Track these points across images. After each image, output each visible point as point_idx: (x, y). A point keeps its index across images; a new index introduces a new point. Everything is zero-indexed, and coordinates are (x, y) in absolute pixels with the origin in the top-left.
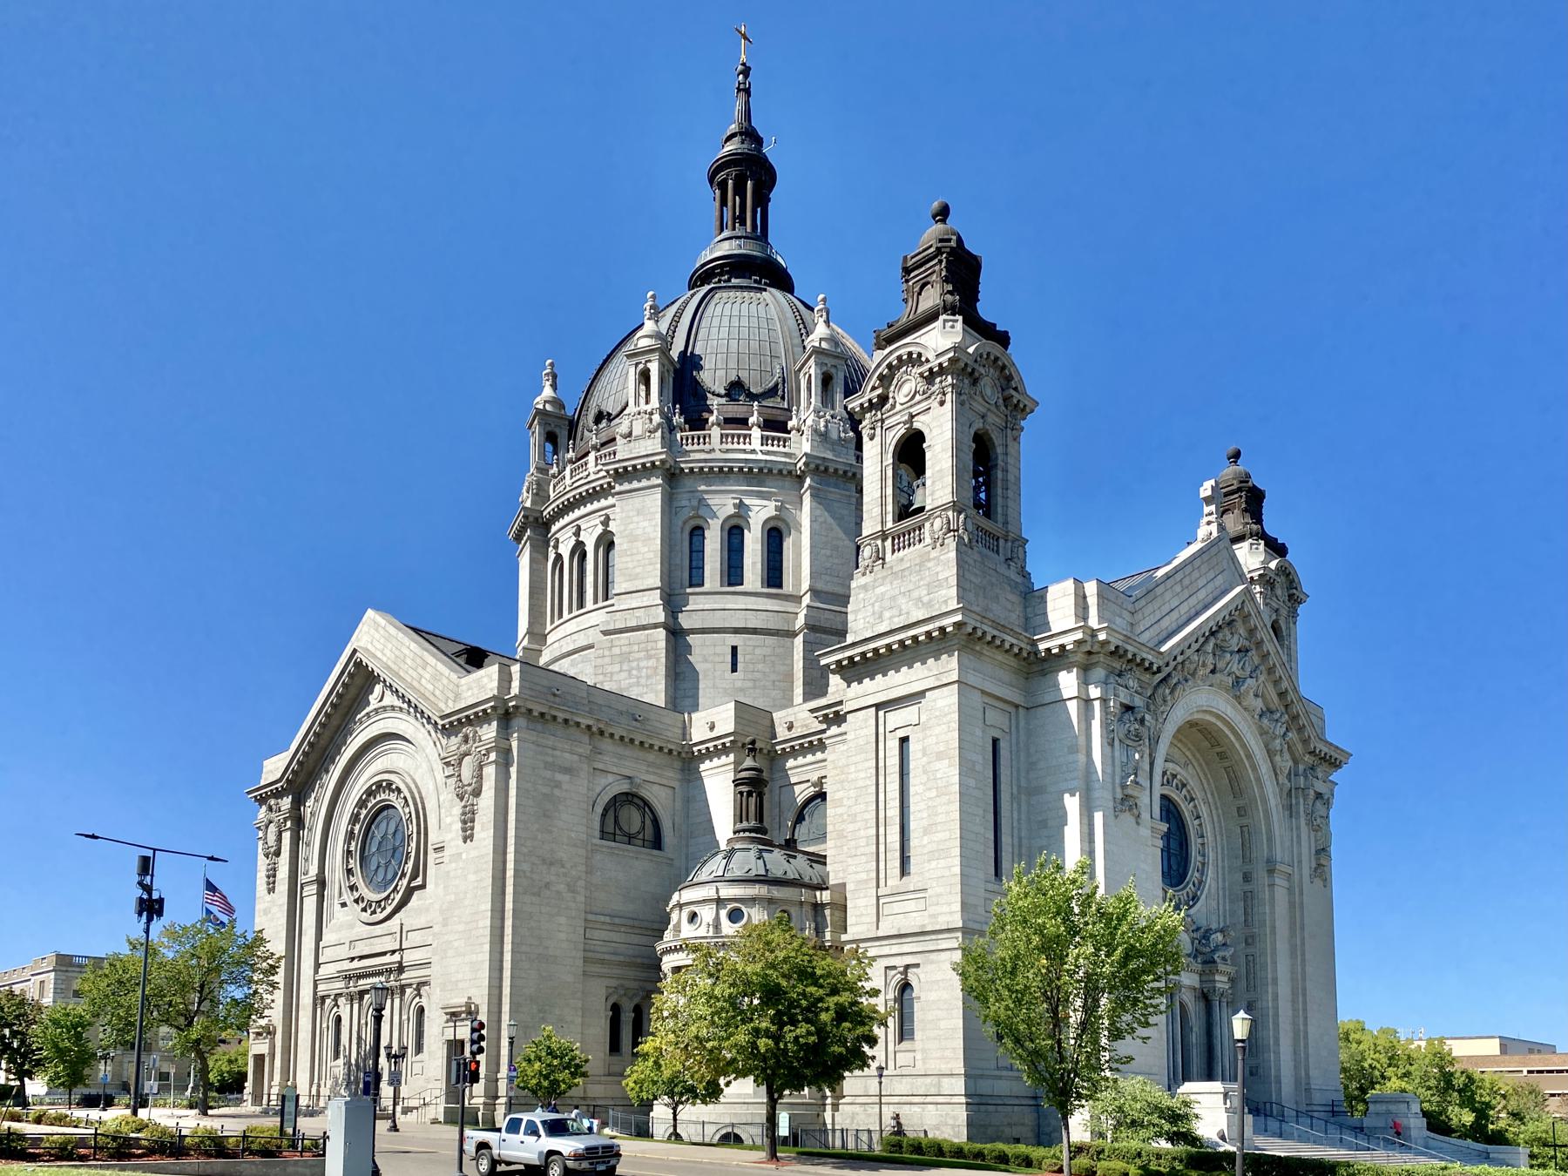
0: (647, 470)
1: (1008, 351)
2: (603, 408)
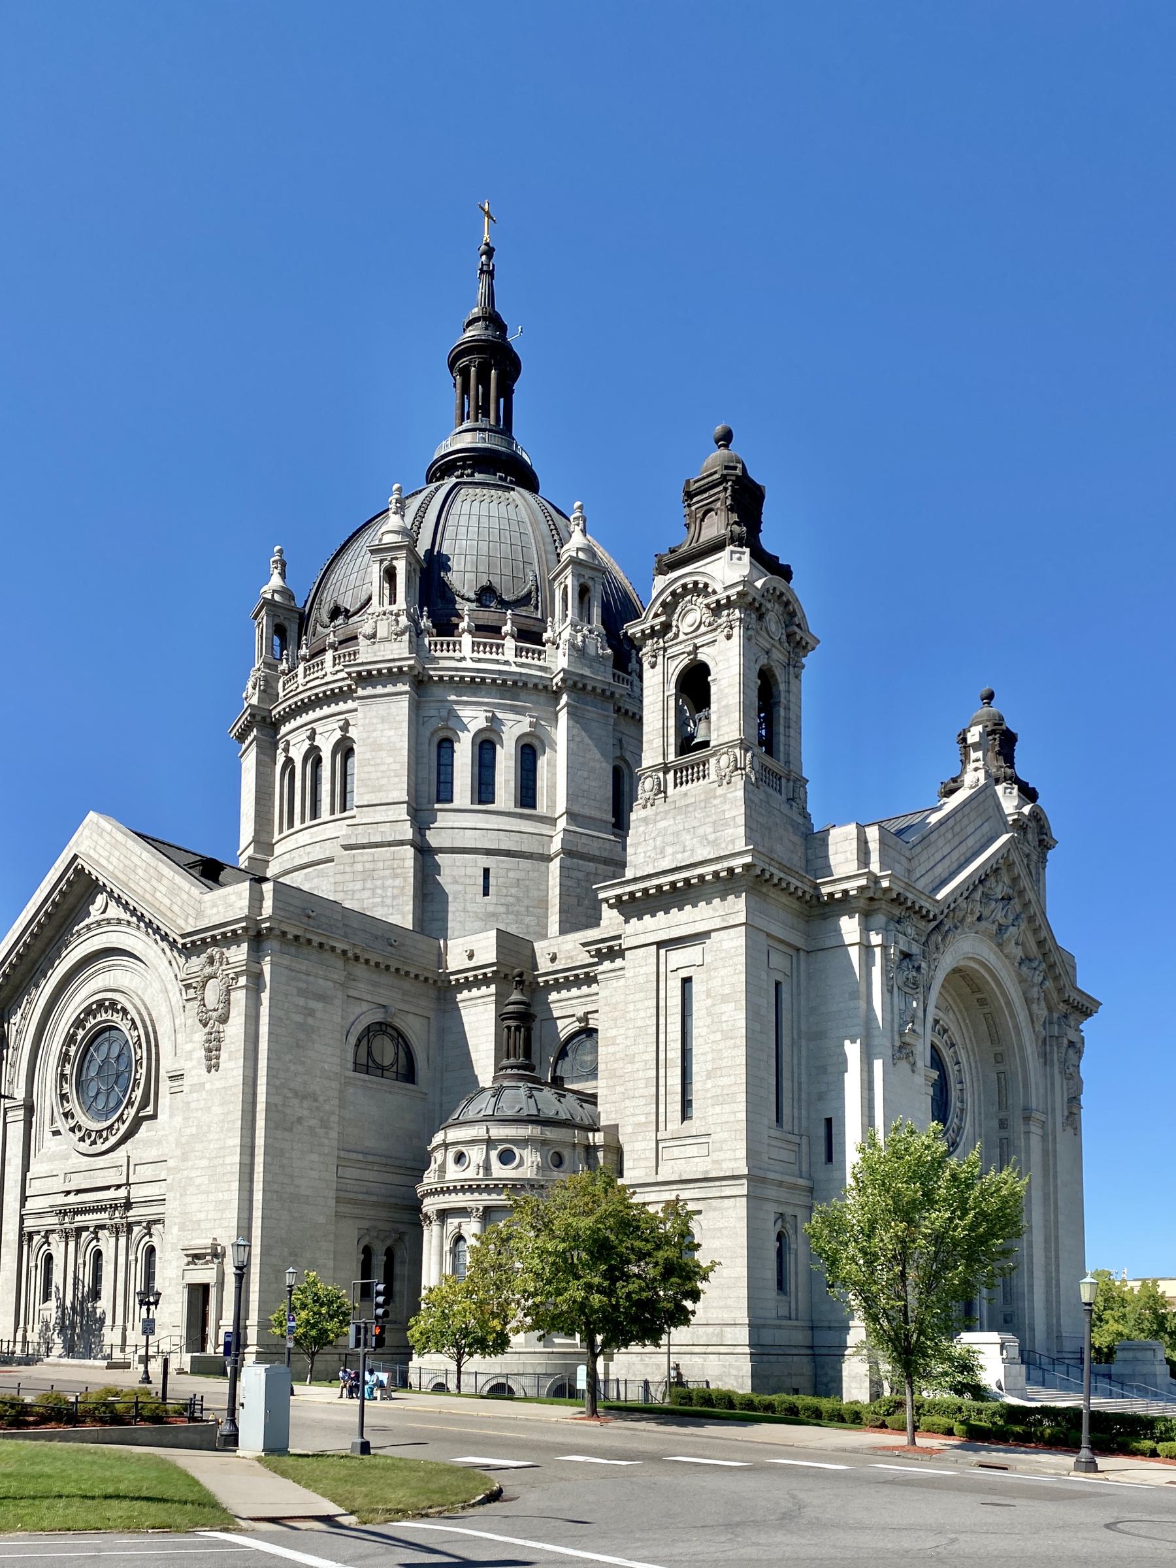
0: (393, 676)
1: (791, 585)
2: (339, 602)
